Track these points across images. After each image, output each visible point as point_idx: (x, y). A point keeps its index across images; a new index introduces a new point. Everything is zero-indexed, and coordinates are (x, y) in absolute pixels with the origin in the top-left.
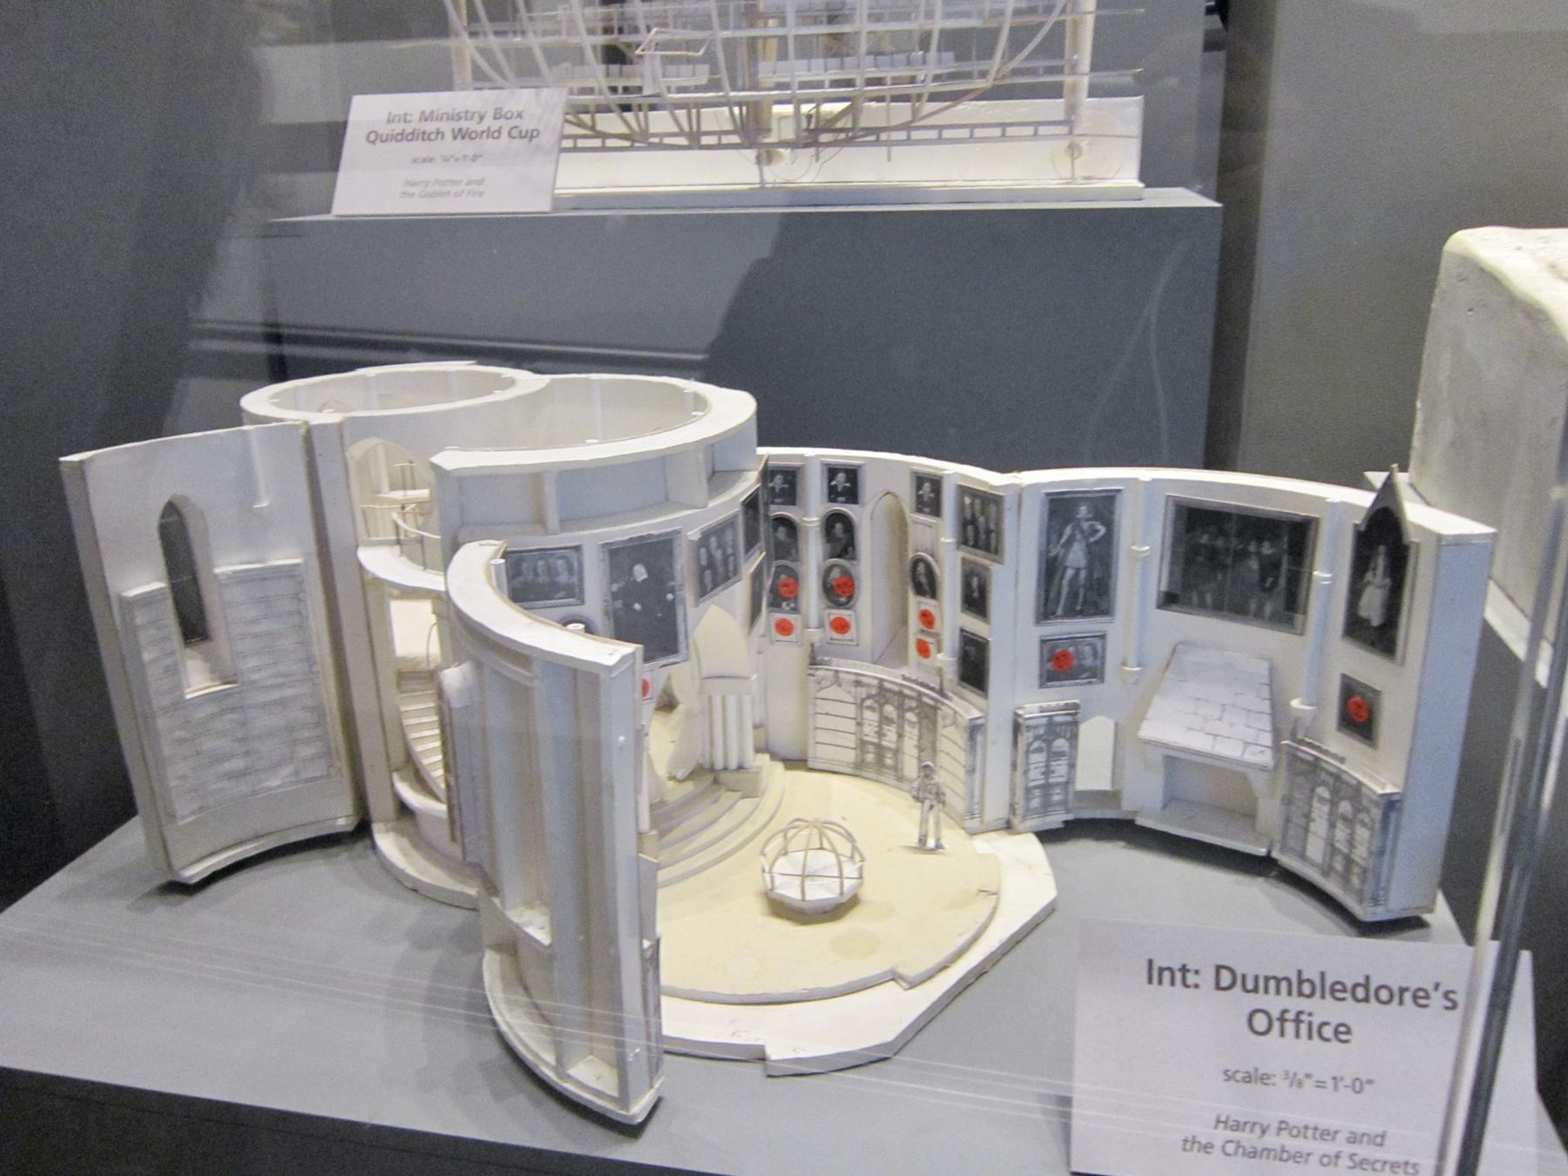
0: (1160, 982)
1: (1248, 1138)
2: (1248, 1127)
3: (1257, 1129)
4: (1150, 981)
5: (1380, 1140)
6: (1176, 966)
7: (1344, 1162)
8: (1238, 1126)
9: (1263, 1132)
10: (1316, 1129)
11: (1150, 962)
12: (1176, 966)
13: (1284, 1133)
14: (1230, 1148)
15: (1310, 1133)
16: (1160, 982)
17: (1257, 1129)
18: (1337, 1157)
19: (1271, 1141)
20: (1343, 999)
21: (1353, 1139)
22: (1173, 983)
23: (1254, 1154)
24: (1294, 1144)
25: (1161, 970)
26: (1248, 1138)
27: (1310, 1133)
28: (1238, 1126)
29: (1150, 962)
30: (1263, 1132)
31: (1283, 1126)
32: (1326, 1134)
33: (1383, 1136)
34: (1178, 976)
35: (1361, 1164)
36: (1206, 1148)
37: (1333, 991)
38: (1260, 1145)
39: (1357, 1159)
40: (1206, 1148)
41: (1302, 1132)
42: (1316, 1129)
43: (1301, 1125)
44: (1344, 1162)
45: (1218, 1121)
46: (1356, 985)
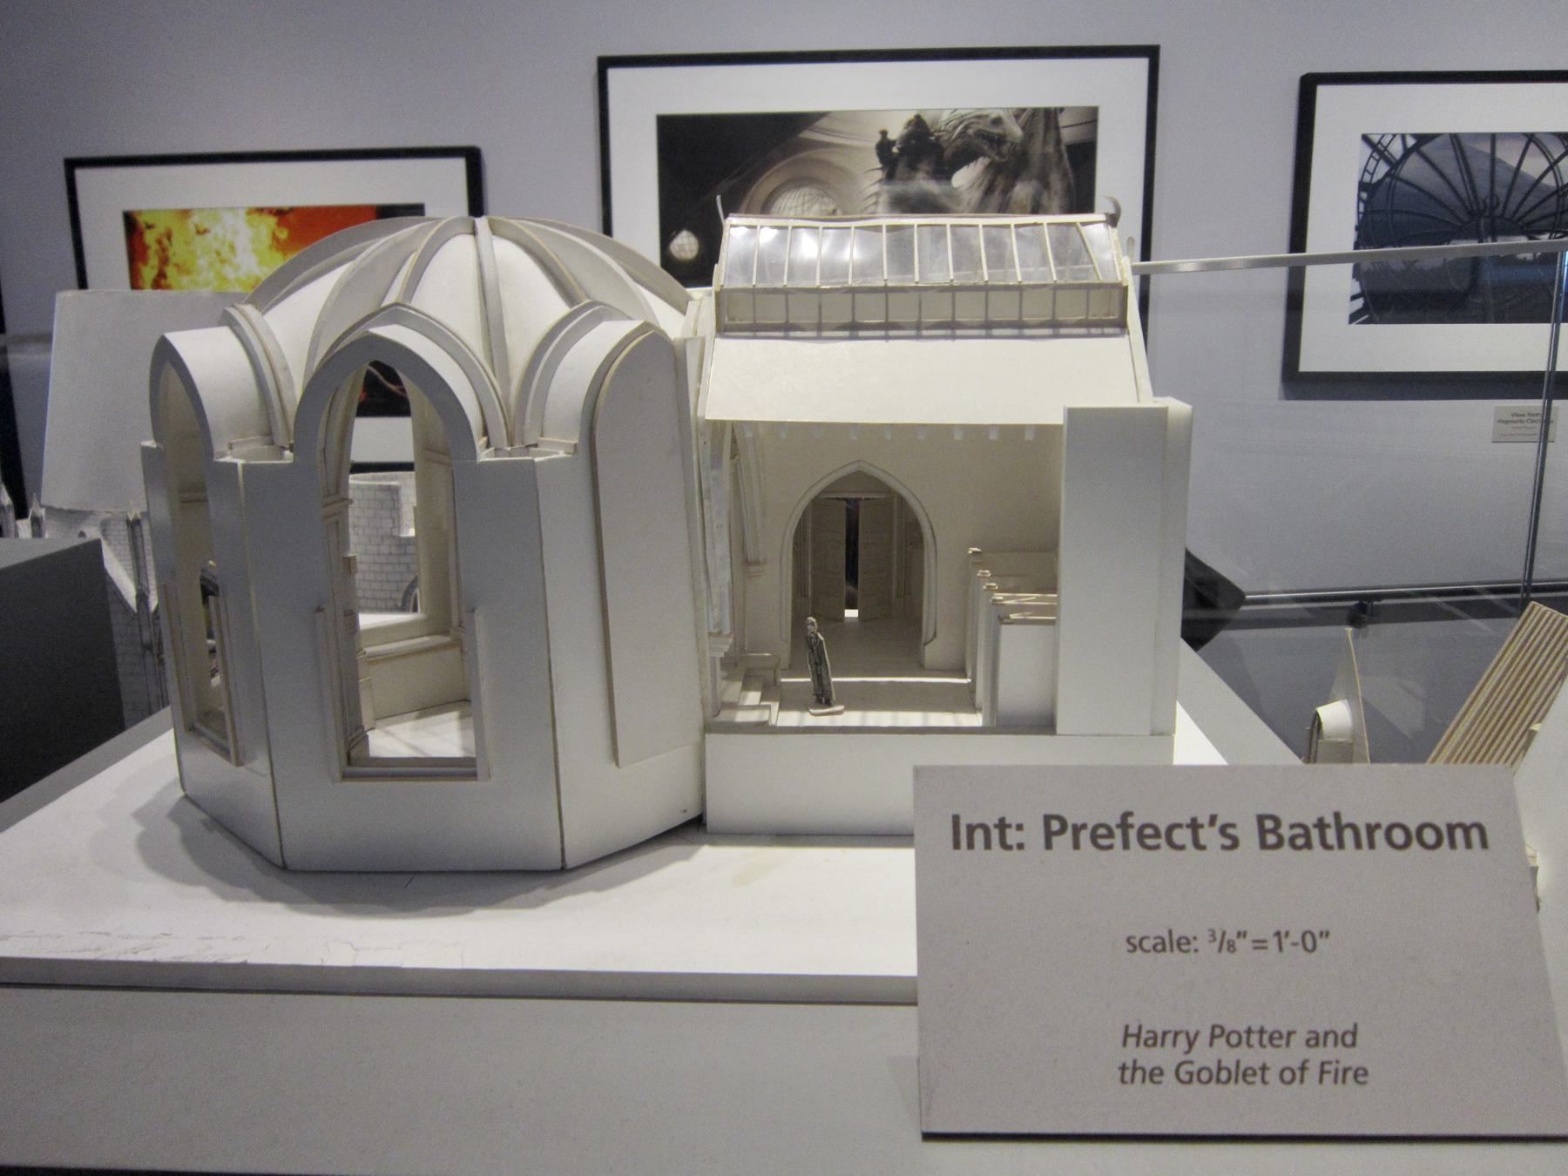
2: (1170, 1037)
3: (1182, 1039)
5: (1349, 1038)
8: (1154, 1040)
9: (1191, 1045)
10: (1262, 1031)
13: (1220, 1043)
15: (1255, 1038)
17: (1182, 1039)
18: (1303, 1068)
19: (1204, 1055)
20: (1157, 847)
21: (1314, 1040)
26: (1165, 1057)
27: (1255, 1038)
28: (1154, 1040)
30: (1191, 1045)
31: (1217, 1032)
32: (1277, 1038)
33: (1354, 1034)
37: (1141, 837)
41: (1244, 1038)
42: (1262, 1031)
43: (1242, 1028)
45: (1127, 1035)
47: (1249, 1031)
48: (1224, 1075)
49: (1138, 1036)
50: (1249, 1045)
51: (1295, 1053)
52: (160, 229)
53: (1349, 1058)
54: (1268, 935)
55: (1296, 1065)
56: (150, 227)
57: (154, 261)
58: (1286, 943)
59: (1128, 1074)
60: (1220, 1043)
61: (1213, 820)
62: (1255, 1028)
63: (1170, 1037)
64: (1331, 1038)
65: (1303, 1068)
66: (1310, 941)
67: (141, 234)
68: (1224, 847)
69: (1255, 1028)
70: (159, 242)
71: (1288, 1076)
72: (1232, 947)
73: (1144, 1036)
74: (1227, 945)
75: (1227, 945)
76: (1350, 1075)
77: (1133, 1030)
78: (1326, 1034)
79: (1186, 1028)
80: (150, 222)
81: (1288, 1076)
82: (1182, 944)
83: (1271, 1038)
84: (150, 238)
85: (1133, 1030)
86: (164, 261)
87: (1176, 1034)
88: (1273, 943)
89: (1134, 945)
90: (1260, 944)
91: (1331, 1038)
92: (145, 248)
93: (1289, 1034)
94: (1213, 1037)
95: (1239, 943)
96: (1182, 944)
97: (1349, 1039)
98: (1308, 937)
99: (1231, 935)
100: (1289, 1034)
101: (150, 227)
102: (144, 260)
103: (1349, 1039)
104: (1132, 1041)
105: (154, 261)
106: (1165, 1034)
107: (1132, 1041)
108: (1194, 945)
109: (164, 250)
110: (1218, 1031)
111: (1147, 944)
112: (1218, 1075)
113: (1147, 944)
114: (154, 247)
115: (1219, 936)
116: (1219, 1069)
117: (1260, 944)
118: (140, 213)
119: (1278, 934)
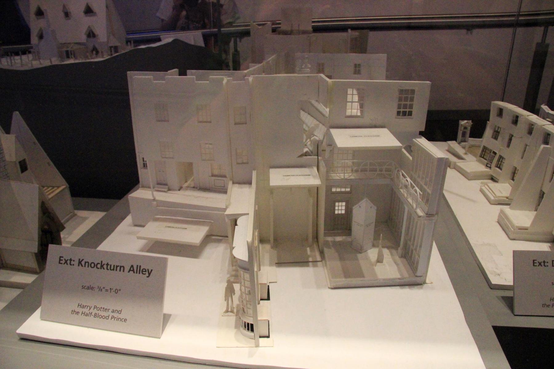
8: (84, 307)
13: (96, 309)
54: (108, 289)
72: (101, 290)
88: (109, 291)
89: (83, 287)
90: (107, 290)
95: (103, 290)
99: (102, 288)
117: (107, 290)
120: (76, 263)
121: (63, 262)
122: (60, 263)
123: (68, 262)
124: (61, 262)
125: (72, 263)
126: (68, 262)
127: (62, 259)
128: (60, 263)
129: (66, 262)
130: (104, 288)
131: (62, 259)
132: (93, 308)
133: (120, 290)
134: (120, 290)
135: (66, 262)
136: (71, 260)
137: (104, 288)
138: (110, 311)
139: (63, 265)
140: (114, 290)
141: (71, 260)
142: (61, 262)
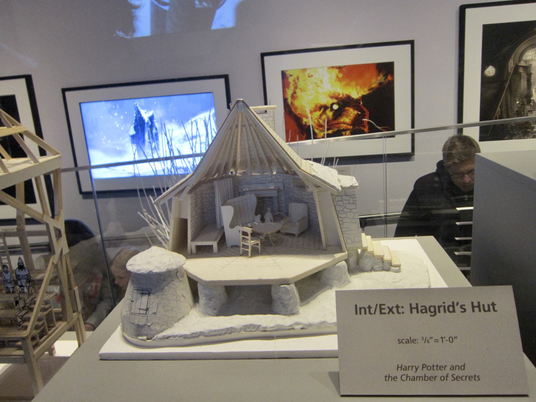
0: (360, 314)
1: (411, 373)
2: (410, 368)
3: (414, 368)
4: (356, 314)
6: (366, 306)
7: (450, 378)
8: (406, 368)
9: (416, 370)
10: (437, 366)
11: (356, 306)
12: (366, 306)
13: (425, 369)
14: (404, 378)
15: (435, 368)
16: (360, 314)
17: (414, 368)
18: (447, 376)
19: (420, 373)
21: (453, 368)
22: (365, 313)
23: (414, 379)
24: (429, 373)
25: (360, 309)
27: (435, 368)
28: (406, 368)
29: (356, 306)
30: (416, 370)
31: (424, 366)
33: (464, 366)
34: (367, 310)
35: (457, 378)
36: (394, 378)
38: (416, 375)
39: (455, 376)
40: (394, 378)
42: (437, 366)
43: (431, 365)
44: (450, 378)
45: (398, 367)
46: (449, 306)
47: (433, 366)
48: (426, 378)
49: (401, 367)
50: (433, 370)
51: (444, 373)
52: (295, 76)
53: (467, 372)
55: (445, 375)
56: (291, 76)
57: (292, 87)
58: (444, 340)
59: (387, 378)
60: (425, 369)
61: (458, 304)
62: (435, 365)
63: (410, 368)
64: (457, 367)
65: (447, 376)
66: (451, 340)
67: (287, 78)
68: (462, 312)
69: (435, 365)
70: (294, 81)
71: (442, 378)
72: (428, 342)
73: (403, 367)
74: (426, 341)
75: (426, 341)
76: (467, 378)
77: (400, 366)
78: (456, 366)
79: (414, 365)
80: (291, 74)
81: (442, 378)
82: (414, 341)
83: (440, 368)
84: (291, 79)
85: (400, 366)
86: (296, 88)
87: (412, 367)
88: (440, 340)
89: (400, 342)
90: (436, 341)
91: (457, 367)
92: (289, 83)
93: (445, 366)
94: (423, 367)
95: (430, 340)
96: (414, 341)
97: (462, 368)
98: (451, 339)
100: (445, 366)
101: (291, 76)
102: (288, 87)
103: (462, 368)
104: (399, 369)
105: (292, 87)
106: (409, 367)
107: (399, 369)
108: (417, 341)
109: (296, 84)
110: (424, 366)
111: (404, 341)
112: (425, 378)
113: (404, 341)
114: (292, 83)
115: (424, 339)
116: (425, 377)
117: (436, 341)
118: (287, 71)
119: (442, 338)
120: (407, 309)
121: (387, 311)
122: (381, 313)
123: (395, 310)
124: (383, 311)
125: (400, 310)
126: (395, 310)
127: (383, 307)
128: (381, 313)
129: (391, 310)
130: (431, 338)
131: (383, 307)
132: (421, 367)
133: (456, 337)
134: (456, 337)
135: (391, 310)
136: (397, 307)
137: (431, 338)
138: (448, 368)
139: (387, 315)
140: (447, 338)
141: (397, 307)
142: (383, 311)
